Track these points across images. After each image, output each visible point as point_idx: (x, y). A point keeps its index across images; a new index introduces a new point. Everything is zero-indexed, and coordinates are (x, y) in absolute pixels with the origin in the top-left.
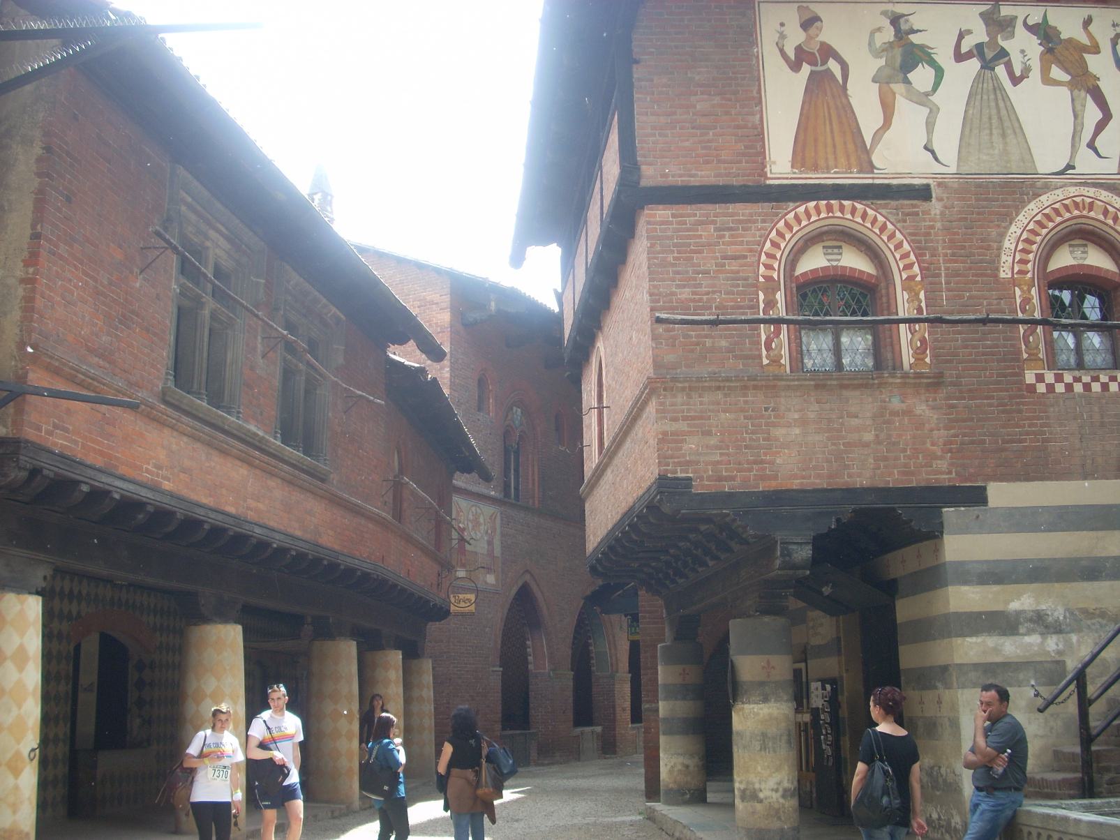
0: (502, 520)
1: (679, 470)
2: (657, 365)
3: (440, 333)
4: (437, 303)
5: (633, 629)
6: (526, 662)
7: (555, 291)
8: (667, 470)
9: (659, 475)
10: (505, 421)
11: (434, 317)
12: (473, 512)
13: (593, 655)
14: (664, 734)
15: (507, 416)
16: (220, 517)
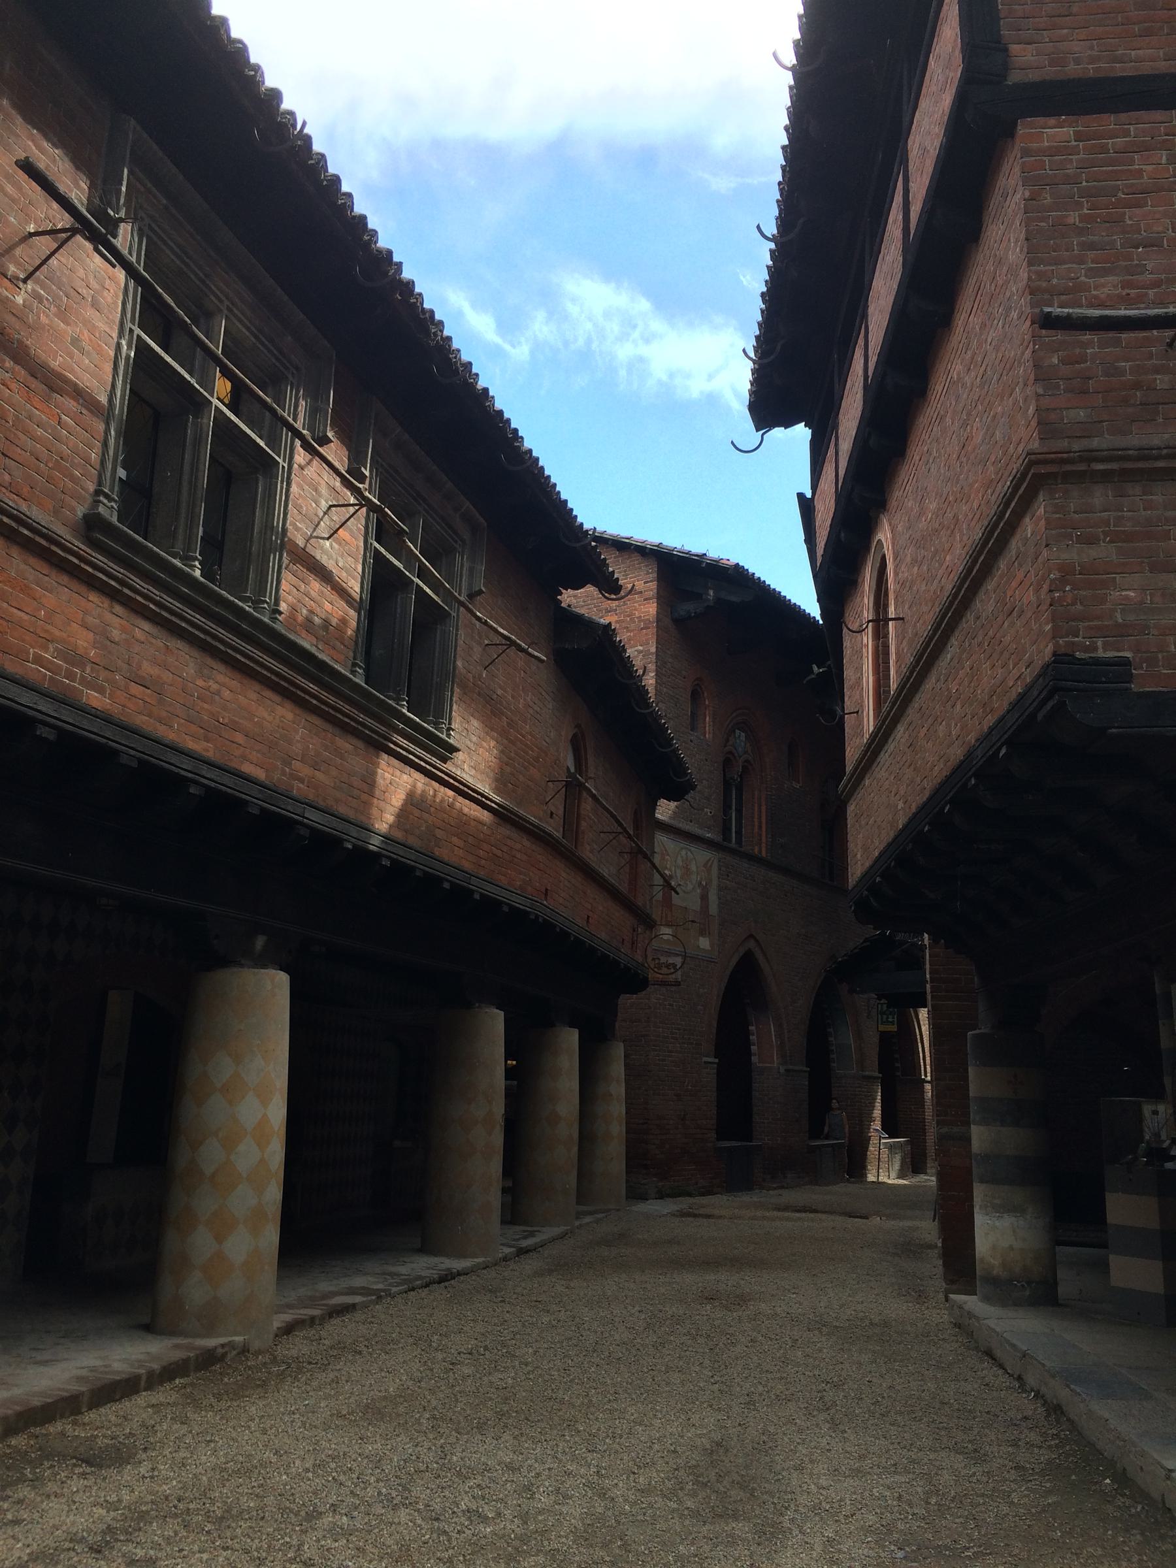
0: (720, 869)
1: (1100, 644)
2: (1046, 426)
3: (642, 629)
4: (641, 592)
5: (885, 1017)
6: (749, 1054)
7: (801, 496)
8: (1073, 643)
9: (1054, 654)
10: (725, 746)
11: (636, 610)
12: (682, 857)
13: (834, 1048)
14: (982, 1181)
15: (727, 740)
16: (228, 780)
